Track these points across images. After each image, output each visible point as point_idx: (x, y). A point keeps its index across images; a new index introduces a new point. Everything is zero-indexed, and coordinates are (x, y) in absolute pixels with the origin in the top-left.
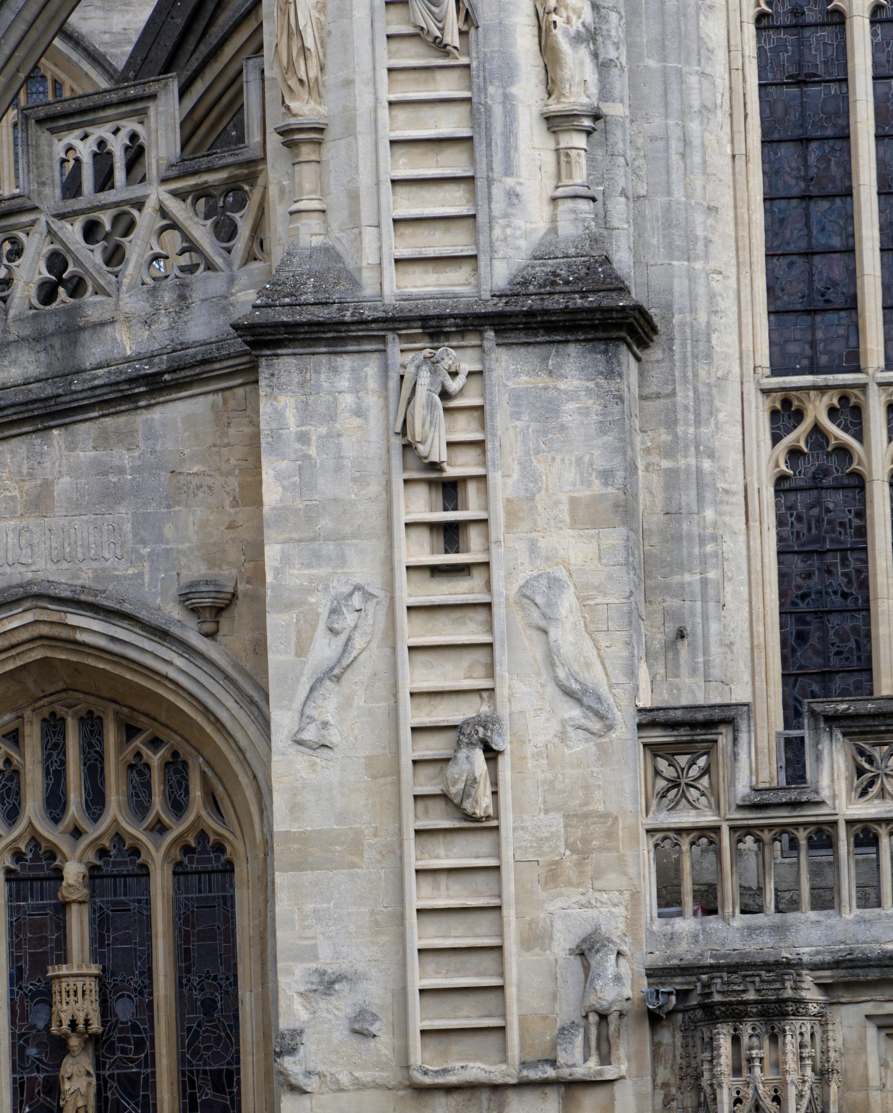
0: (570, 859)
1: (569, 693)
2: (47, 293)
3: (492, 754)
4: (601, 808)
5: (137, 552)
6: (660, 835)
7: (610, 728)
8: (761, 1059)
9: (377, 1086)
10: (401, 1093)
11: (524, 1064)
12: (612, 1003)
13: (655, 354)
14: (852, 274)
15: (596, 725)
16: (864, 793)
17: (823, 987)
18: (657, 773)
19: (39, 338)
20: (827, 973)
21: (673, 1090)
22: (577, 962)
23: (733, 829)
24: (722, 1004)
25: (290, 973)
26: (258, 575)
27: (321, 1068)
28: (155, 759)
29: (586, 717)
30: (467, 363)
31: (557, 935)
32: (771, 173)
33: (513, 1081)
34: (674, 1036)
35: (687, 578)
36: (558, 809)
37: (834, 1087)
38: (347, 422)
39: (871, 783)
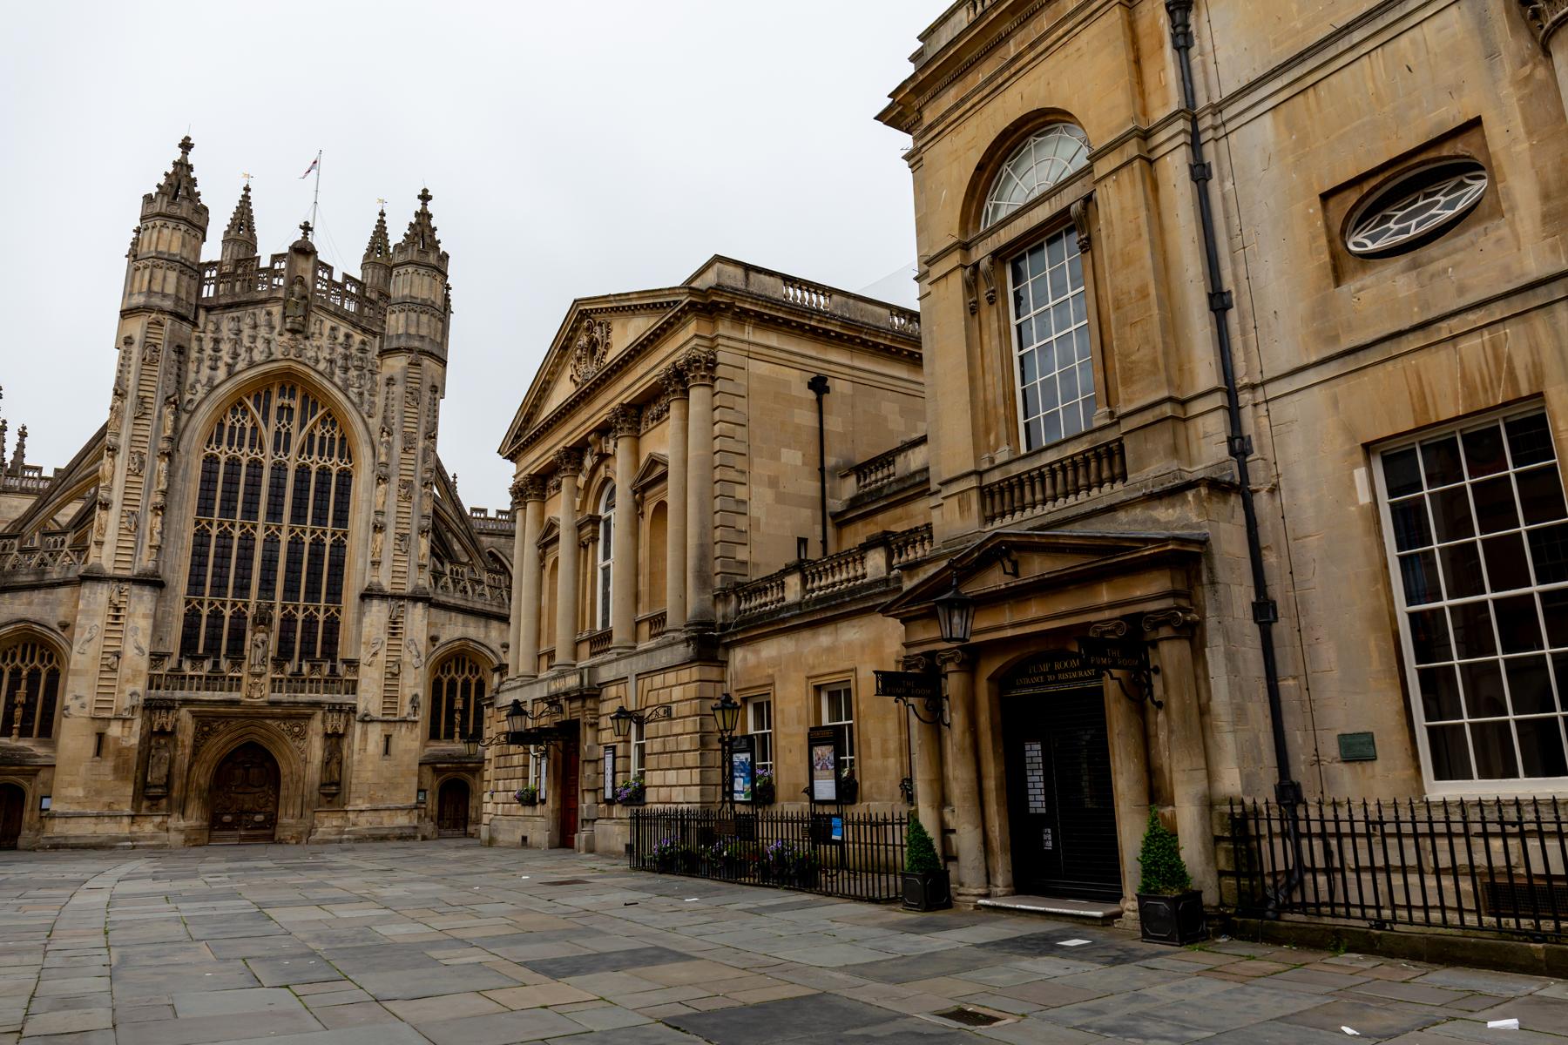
2: (40, 565)
3: (118, 658)
13: (164, 590)
14: (205, 580)
19: (36, 574)
26: (75, 621)
28: (47, 653)
30: (126, 587)
32: (192, 561)
38: (99, 595)
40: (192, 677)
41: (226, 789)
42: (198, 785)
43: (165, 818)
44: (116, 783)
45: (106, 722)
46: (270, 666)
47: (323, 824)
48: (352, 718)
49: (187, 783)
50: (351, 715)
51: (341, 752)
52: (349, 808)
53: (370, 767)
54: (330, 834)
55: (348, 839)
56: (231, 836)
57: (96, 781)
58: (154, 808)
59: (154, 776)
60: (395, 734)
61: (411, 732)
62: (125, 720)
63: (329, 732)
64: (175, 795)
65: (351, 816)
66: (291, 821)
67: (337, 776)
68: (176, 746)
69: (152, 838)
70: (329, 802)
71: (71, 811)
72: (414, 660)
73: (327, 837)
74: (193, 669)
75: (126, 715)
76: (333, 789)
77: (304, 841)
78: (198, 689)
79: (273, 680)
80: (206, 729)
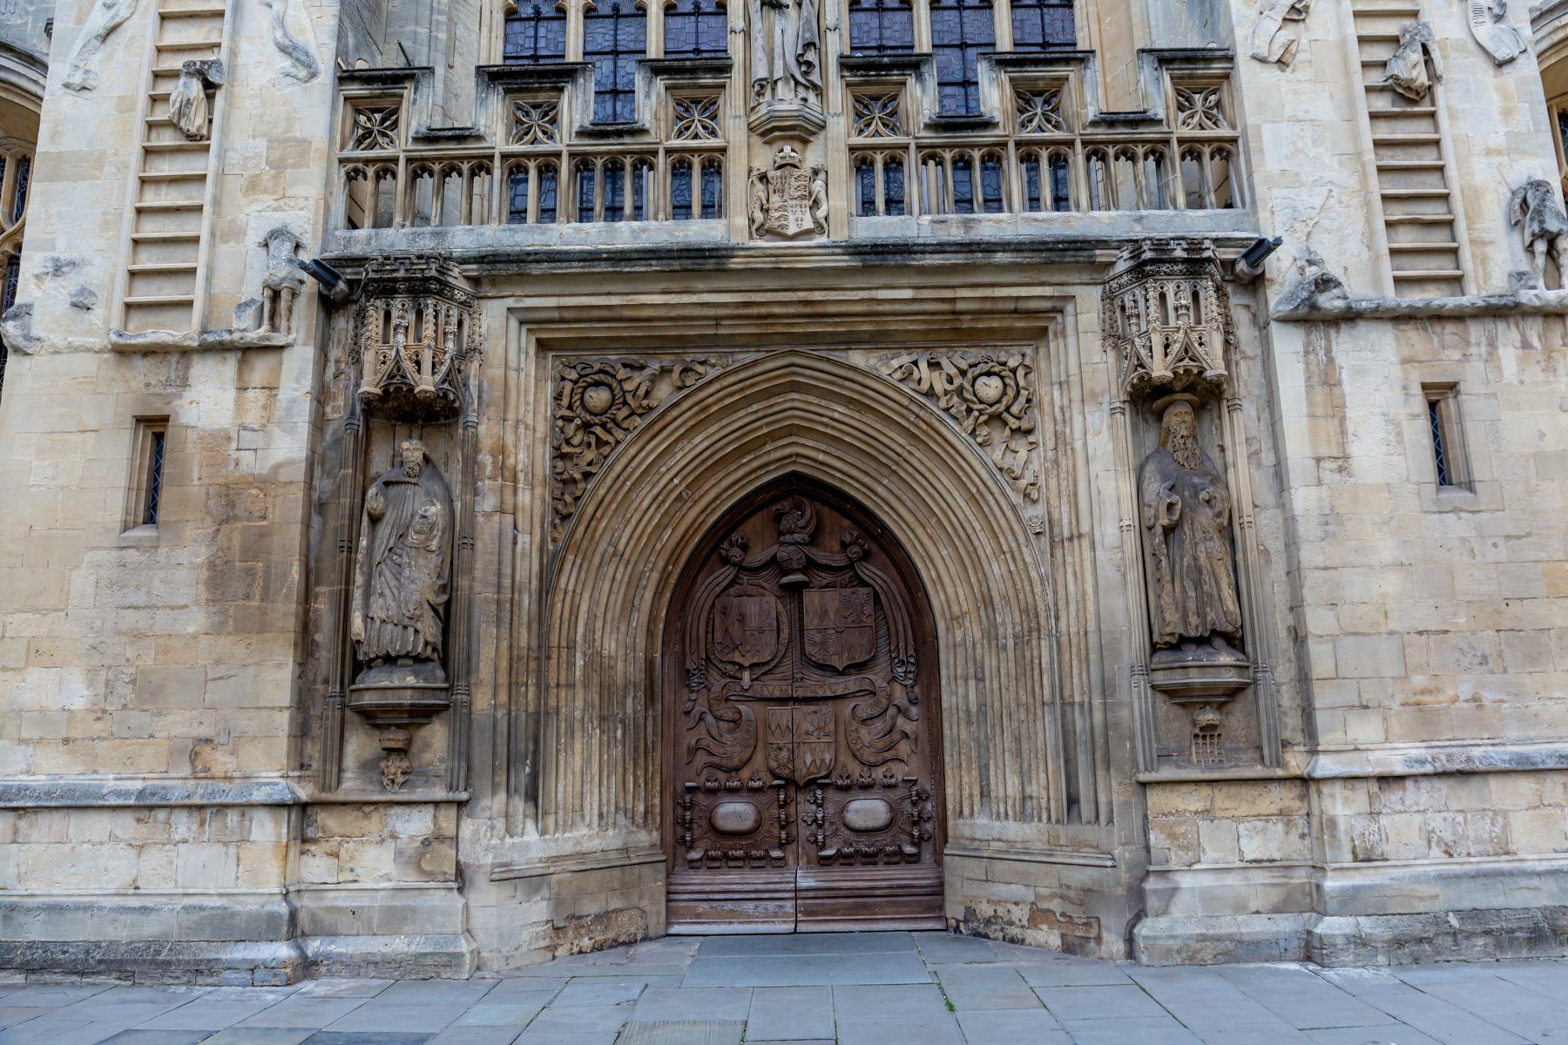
0: (268, 173)
1: (283, 49)
4: (298, 134)
5: (26, 9)
6: (351, 166)
7: (313, 75)
8: (407, 328)
9: (88, 350)
10: (106, 356)
11: (204, 331)
12: (283, 279)
15: (303, 73)
16: (521, 139)
17: (475, 281)
18: (356, 123)
20: (474, 266)
21: (343, 366)
22: (263, 251)
23: (409, 160)
24: (375, 280)
25: (30, 259)
27: (42, 334)
29: (295, 66)
31: (250, 232)
33: (195, 344)
34: (348, 322)
35: (420, 30)
36: (264, 135)
37: (476, 364)
39: (527, 133)
40: (515, 169)
41: (717, 682)
42: (597, 662)
43: (447, 819)
44: (224, 644)
45: (171, 367)
46: (837, 94)
47: (1194, 847)
48: (1241, 317)
49: (543, 651)
50: (1236, 300)
51: (1219, 479)
52: (1325, 766)
53: (1386, 550)
54: (1240, 908)
55: (1359, 942)
56: (757, 896)
57: (137, 636)
58: (395, 766)
59: (377, 611)
60: (1473, 378)
61: (1550, 368)
62: (247, 351)
63: (1160, 369)
64: (482, 702)
65: (1341, 806)
66: (1014, 830)
67: (1231, 605)
68: (471, 467)
69: (394, 919)
70: (1208, 732)
71: (39, 780)
72: (1486, 31)
73: (1228, 925)
74: (519, 128)
75: (249, 329)
76: (1222, 665)
77: (1114, 944)
78: (548, 214)
79: (861, 163)
80: (599, 397)
